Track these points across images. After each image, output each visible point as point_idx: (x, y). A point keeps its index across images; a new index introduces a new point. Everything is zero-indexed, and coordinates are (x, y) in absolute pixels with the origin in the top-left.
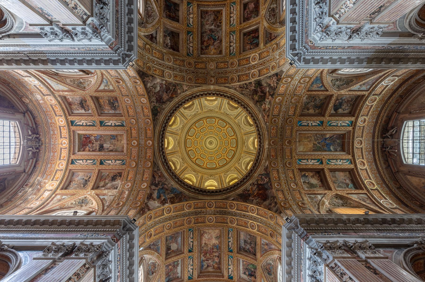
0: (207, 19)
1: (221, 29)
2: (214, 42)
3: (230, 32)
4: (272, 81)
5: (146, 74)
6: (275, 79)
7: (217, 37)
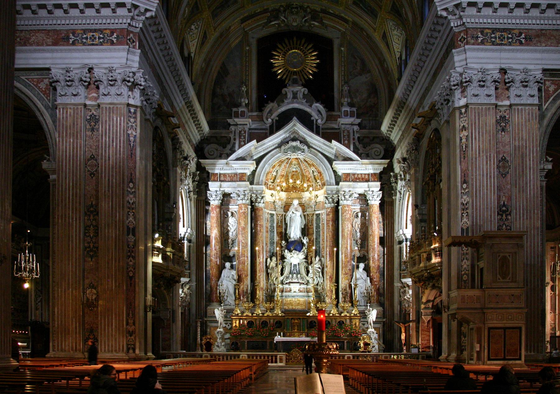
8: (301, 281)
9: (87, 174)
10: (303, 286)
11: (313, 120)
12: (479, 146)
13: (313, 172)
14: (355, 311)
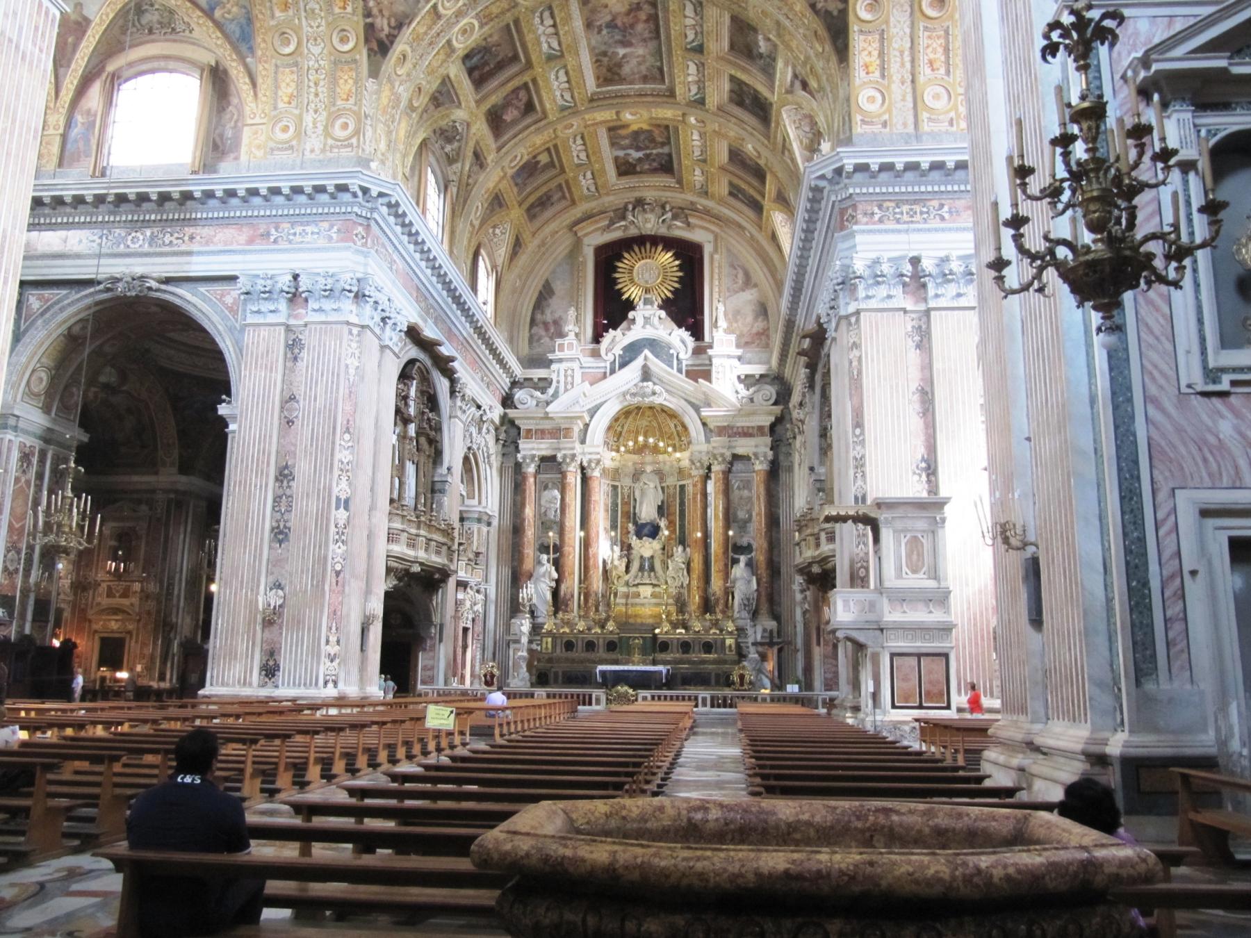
0: (643, 68)
1: (592, 49)
2: (613, 20)
3: (562, 56)
4: (386, 13)
5: (829, 28)
6: (383, 24)
7: (604, 32)
8: (654, 582)
9: (284, 421)
10: (657, 589)
12: (879, 372)
14: (731, 627)
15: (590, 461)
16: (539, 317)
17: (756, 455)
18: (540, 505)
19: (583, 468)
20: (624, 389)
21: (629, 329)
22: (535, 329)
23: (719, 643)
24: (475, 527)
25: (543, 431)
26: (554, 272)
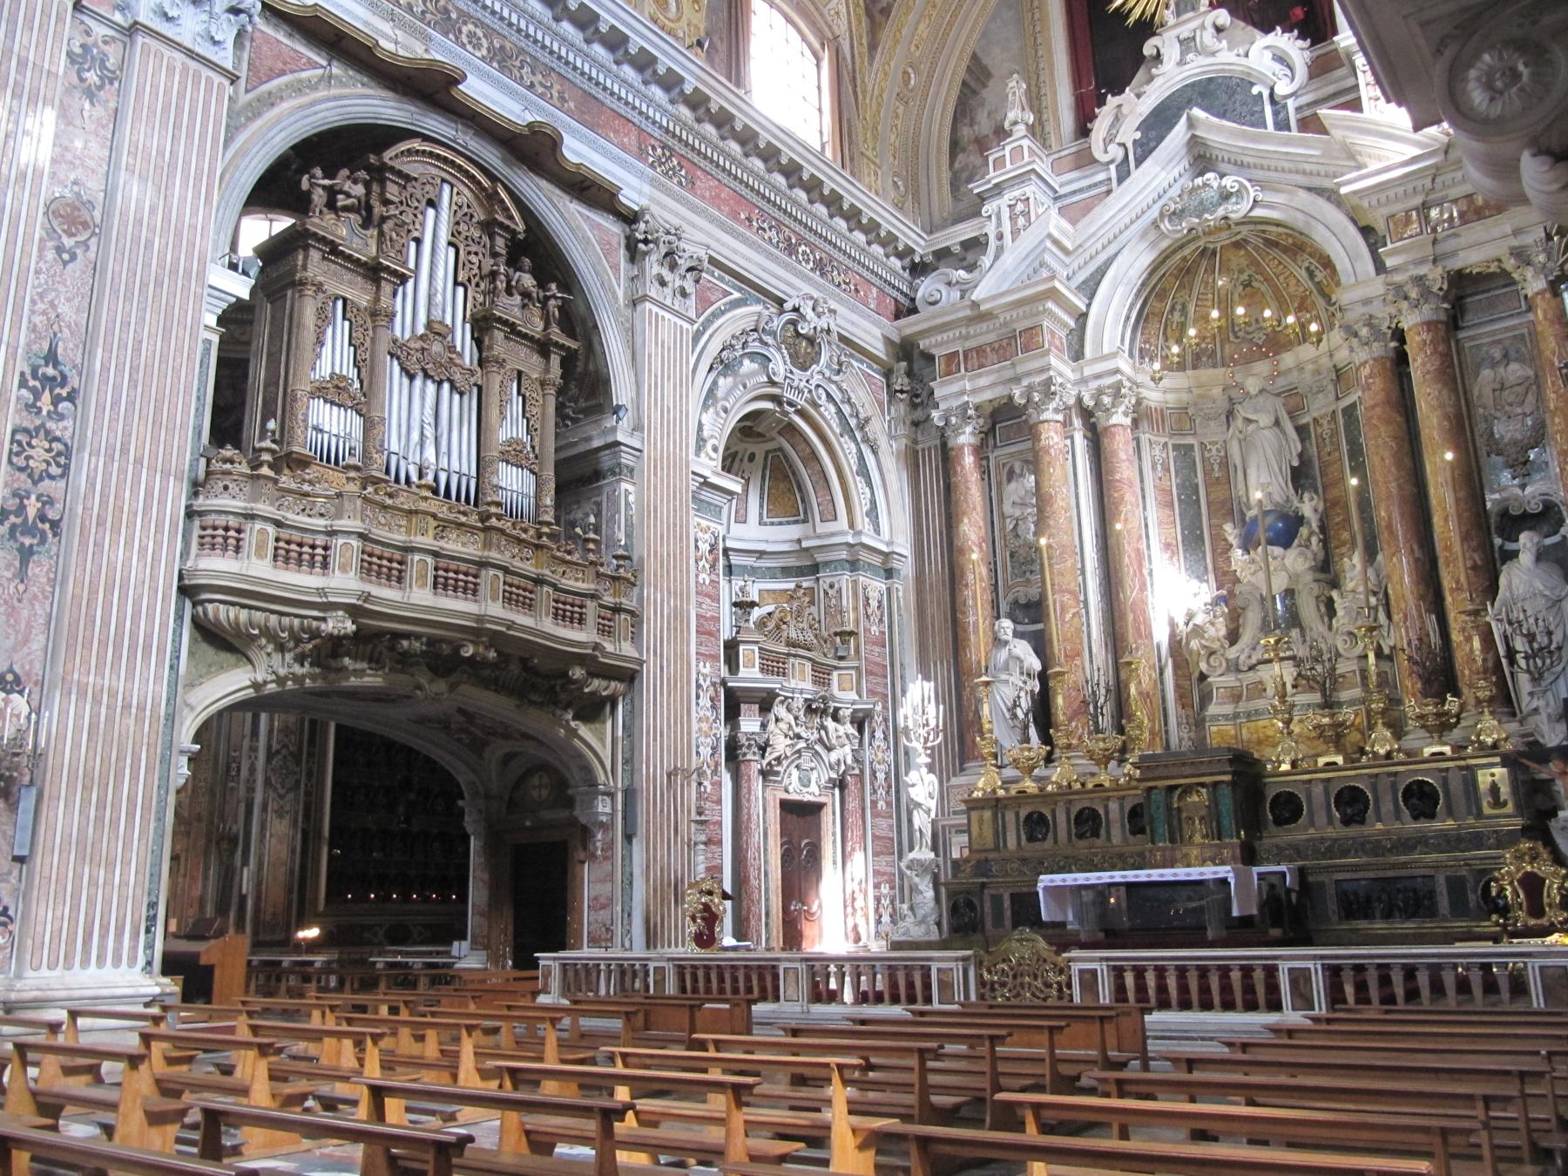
11: (1260, 94)
13: (1311, 274)
15: (1100, 392)
16: (966, 132)
17: (1521, 255)
18: (1003, 517)
19: (1087, 414)
20: (1154, 213)
21: (1151, 79)
22: (961, 157)
23: (1456, 784)
24: (845, 580)
25: (980, 350)
26: (984, 35)
